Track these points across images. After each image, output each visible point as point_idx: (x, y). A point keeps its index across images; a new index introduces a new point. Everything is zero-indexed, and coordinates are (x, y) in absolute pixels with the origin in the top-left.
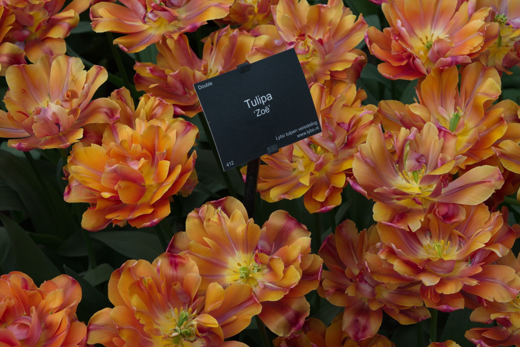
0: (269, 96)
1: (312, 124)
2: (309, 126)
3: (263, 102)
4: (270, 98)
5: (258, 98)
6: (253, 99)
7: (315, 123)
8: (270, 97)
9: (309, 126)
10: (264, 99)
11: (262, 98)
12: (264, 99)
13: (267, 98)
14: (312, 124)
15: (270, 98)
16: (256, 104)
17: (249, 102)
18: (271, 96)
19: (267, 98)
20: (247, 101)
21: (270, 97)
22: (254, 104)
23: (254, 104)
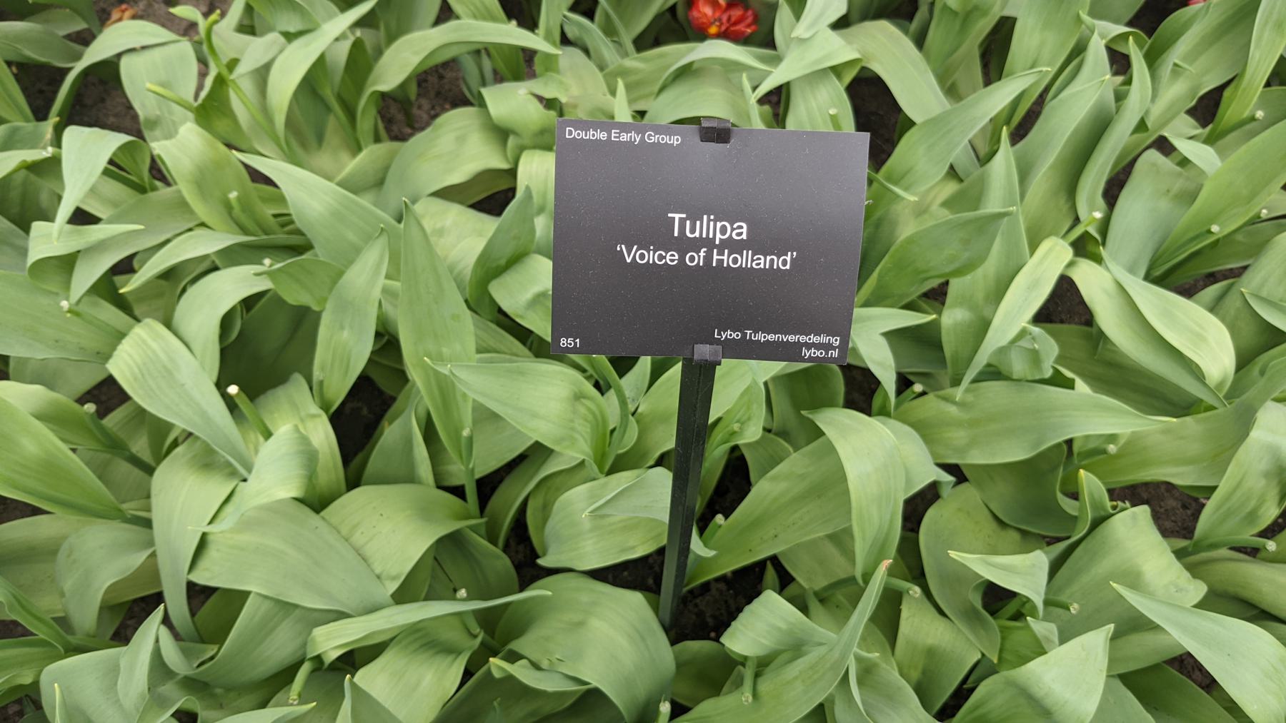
0: (741, 227)
1: (823, 339)
2: (814, 339)
3: (718, 236)
5: (709, 220)
6: (694, 217)
7: (832, 340)
8: (741, 231)
9: (814, 339)
13: (733, 229)
14: (823, 339)
17: (682, 221)
18: (744, 230)
19: (733, 229)
20: (677, 216)
22: (693, 231)
23: (693, 231)
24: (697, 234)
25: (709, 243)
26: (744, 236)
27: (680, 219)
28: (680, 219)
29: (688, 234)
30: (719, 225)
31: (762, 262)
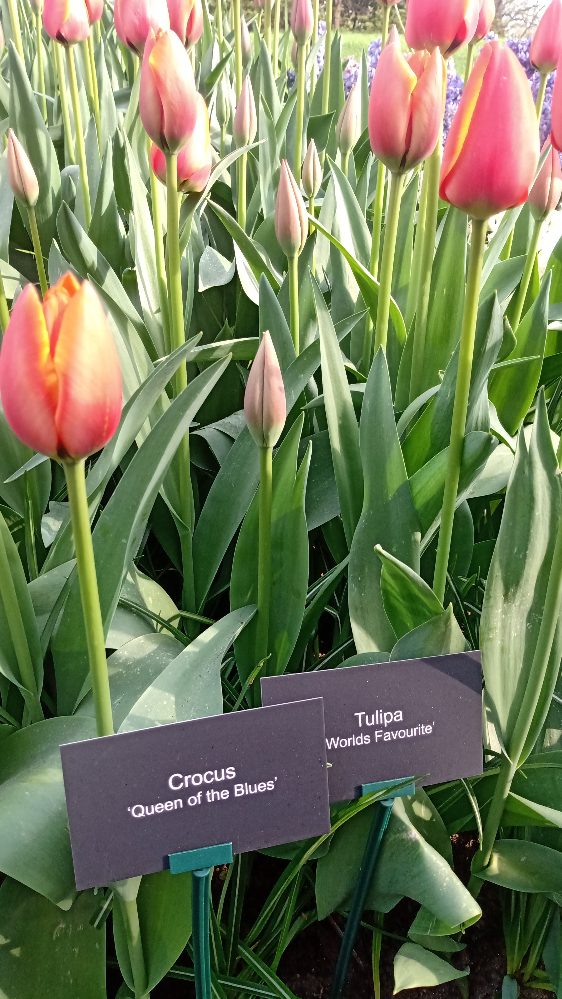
3: (386, 721)
4: (397, 718)
5: (379, 713)
6: (370, 713)
8: (399, 716)
10: (388, 717)
11: (386, 714)
12: (388, 717)
13: (394, 716)
15: (399, 717)
16: (373, 723)
17: (363, 717)
18: (401, 715)
19: (394, 716)
20: (360, 714)
21: (399, 716)
22: (370, 721)
23: (370, 721)
24: (373, 723)
25: (380, 727)
26: (401, 719)
27: (362, 715)
28: (362, 715)
29: (368, 724)
30: (386, 714)
31: (413, 732)
